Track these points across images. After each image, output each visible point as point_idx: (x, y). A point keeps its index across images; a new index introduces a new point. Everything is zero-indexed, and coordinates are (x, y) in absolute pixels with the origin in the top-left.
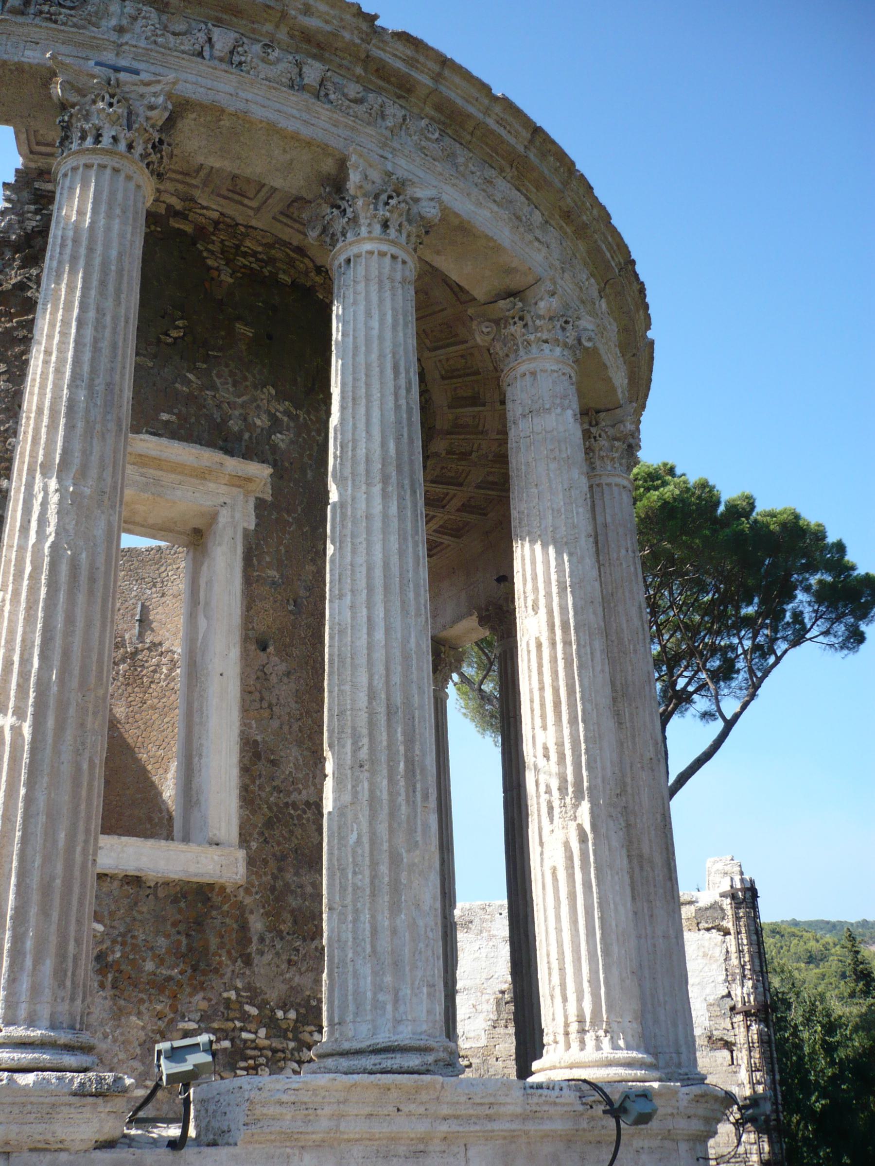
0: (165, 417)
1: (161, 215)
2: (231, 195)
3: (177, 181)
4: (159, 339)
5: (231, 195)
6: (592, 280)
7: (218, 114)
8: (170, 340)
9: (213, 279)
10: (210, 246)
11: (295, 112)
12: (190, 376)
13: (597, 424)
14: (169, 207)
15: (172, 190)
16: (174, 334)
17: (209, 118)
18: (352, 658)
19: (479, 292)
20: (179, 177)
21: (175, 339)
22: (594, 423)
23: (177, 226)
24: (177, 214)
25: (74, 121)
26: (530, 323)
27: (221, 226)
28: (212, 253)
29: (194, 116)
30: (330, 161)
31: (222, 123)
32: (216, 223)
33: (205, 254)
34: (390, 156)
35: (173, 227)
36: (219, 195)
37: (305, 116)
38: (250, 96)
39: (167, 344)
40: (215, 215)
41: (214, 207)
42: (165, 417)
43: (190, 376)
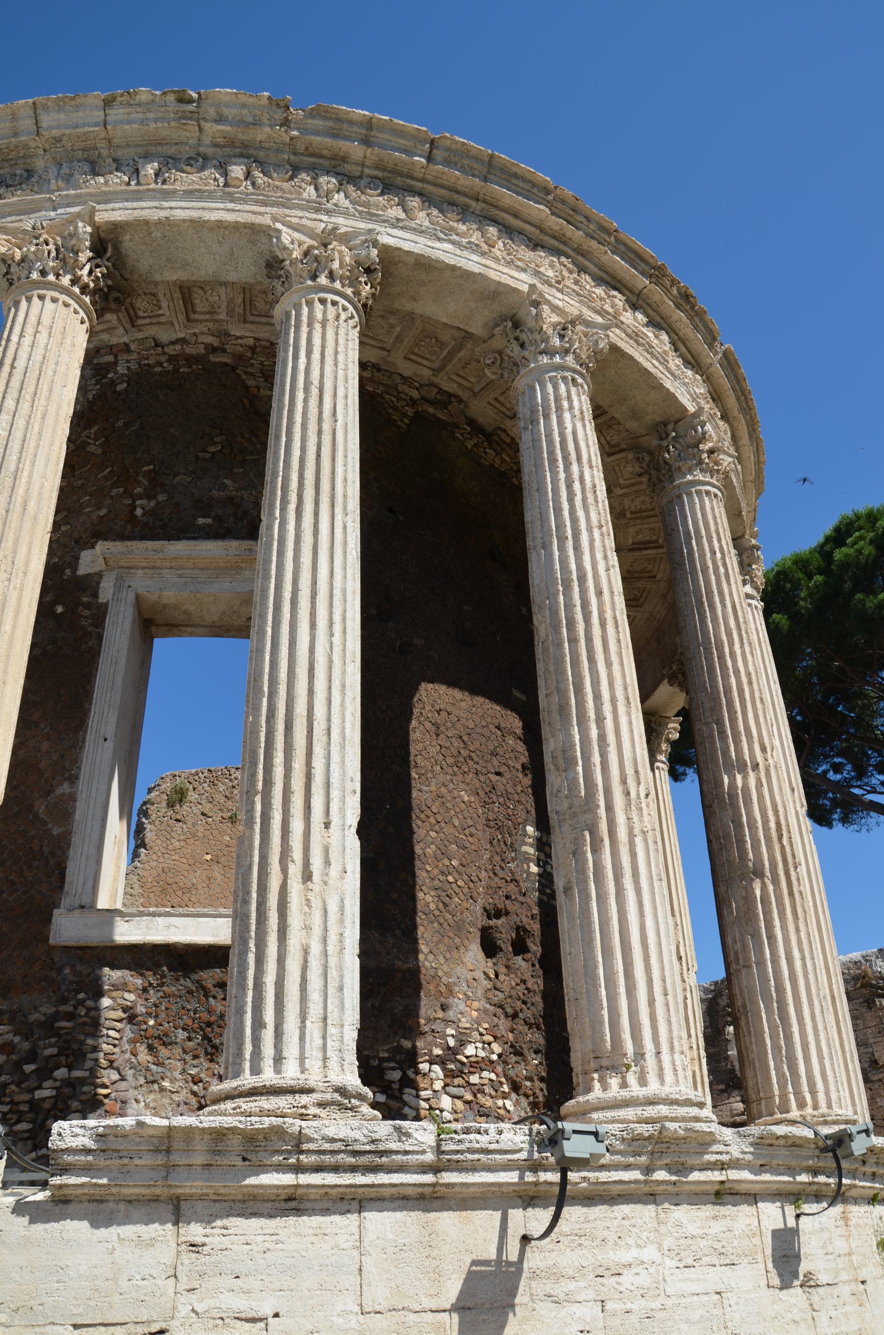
0: (201, 521)
1: (203, 356)
2: (257, 319)
3: (207, 321)
4: (197, 457)
5: (257, 319)
6: (615, 293)
7: (145, 227)
8: (208, 455)
9: (254, 396)
10: (250, 370)
11: (222, 206)
12: (226, 481)
13: (667, 435)
14: (206, 345)
15: (205, 330)
16: (213, 449)
17: (141, 235)
18: (255, 681)
19: (476, 328)
20: (207, 317)
21: (213, 453)
22: (664, 435)
23: (217, 360)
24: (214, 350)
25: (12, 270)
26: (526, 341)
27: (258, 350)
28: (251, 374)
29: (128, 237)
30: (264, 239)
31: (154, 235)
32: (253, 349)
33: (244, 377)
34: (325, 218)
35: (215, 363)
36: (245, 322)
37: (230, 205)
38: (173, 204)
39: (204, 459)
40: (251, 342)
41: (247, 334)
42: (201, 521)
43: (226, 481)
